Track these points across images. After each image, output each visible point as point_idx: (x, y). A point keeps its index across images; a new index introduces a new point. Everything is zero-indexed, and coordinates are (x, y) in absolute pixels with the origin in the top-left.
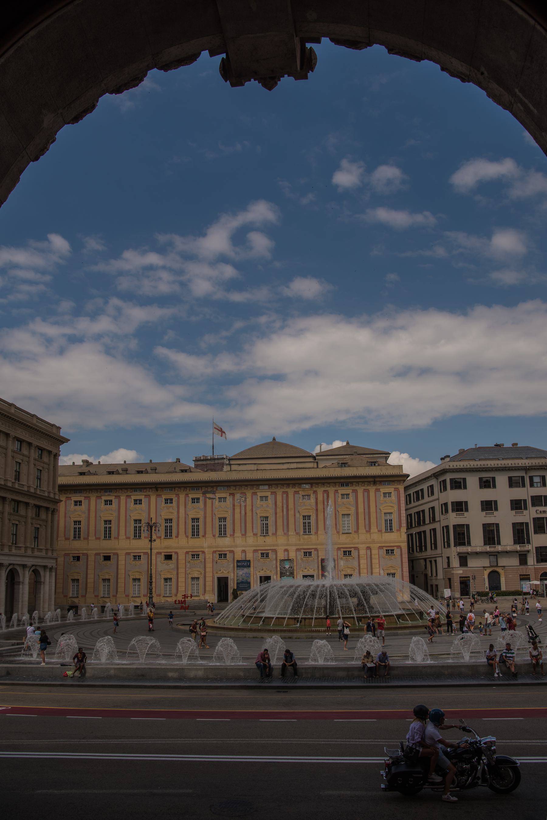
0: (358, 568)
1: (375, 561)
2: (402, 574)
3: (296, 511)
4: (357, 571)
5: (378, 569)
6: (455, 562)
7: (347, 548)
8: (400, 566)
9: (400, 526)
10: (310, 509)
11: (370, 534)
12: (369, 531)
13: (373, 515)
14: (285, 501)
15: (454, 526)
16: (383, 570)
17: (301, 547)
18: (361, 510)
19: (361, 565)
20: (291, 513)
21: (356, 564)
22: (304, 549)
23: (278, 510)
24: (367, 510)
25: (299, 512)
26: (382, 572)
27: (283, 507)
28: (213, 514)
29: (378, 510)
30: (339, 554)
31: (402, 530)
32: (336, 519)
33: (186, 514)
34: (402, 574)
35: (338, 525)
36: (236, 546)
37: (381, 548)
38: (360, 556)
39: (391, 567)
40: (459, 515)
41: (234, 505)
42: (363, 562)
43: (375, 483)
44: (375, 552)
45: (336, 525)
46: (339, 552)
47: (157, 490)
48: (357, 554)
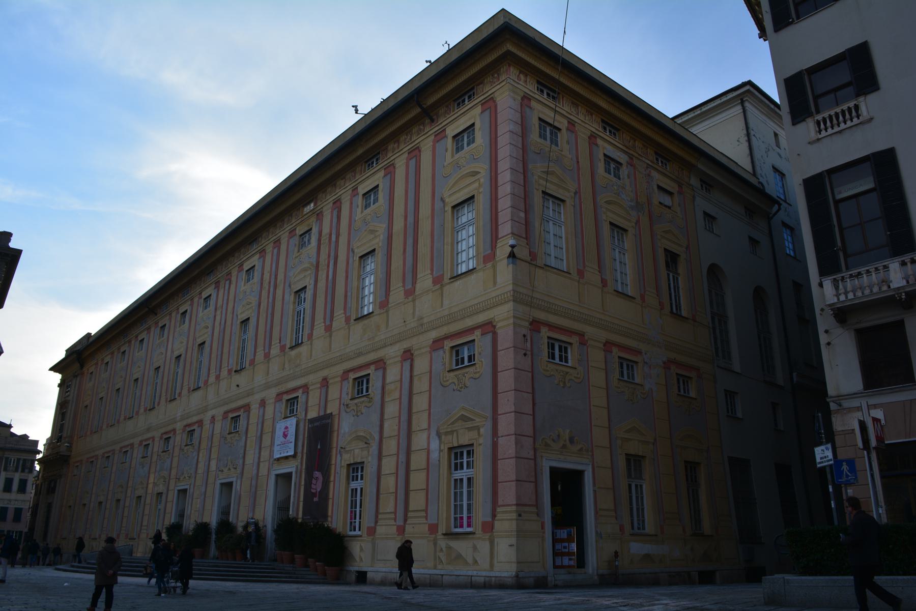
0: (377, 437)
1: (421, 403)
2: (495, 445)
3: (287, 285)
4: (374, 448)
5: (424, 435)
6: (841, 368)
7: (360, 368)
8: (489, 413)
9: (495, 238)
10: (305, 270)
11: (414, 300)
12: (410, 293)
13: (425, 227)
14: (274, 265)
15: (816, 186)
16: (439, 435)
17: (283, 388)
18: (398, 225)
19: (386, 425)
20: (279, 292)
21: (375, 418)
22: (287, 392)
23: (263, 292)
24: (411, 219)
25: (290, 286)
26: (435, 445)
27: (270, 283)
28: (195, 339)
29: (439, 204)
30: (344, 395)
31: (498, 252)
32: (347, 277)
33: (172, 352)
34: (495, 445)
35: (349, 294)
36: (205, 410)
37: (437, 344)
38: (387, 388)
39: (464, 418)
40: (834, 120)
41: (216, 309)
42: (391, 409)
43: (429, 115)
44: (421, 364)
45: (346, 296)
46: (345, 383)
47: (156, 314)
48: (379, 384)
